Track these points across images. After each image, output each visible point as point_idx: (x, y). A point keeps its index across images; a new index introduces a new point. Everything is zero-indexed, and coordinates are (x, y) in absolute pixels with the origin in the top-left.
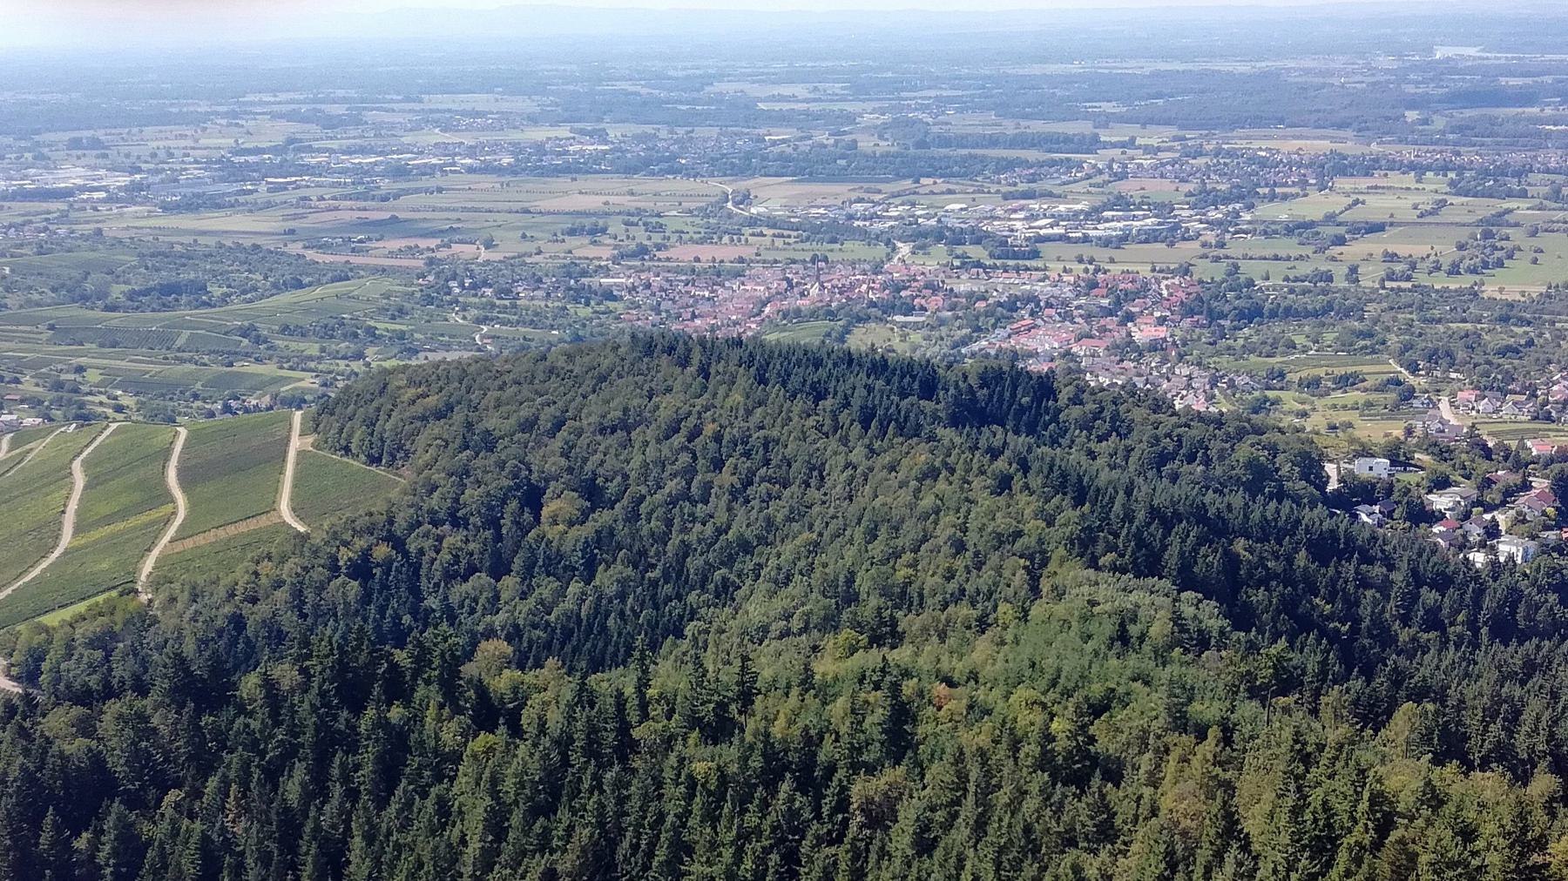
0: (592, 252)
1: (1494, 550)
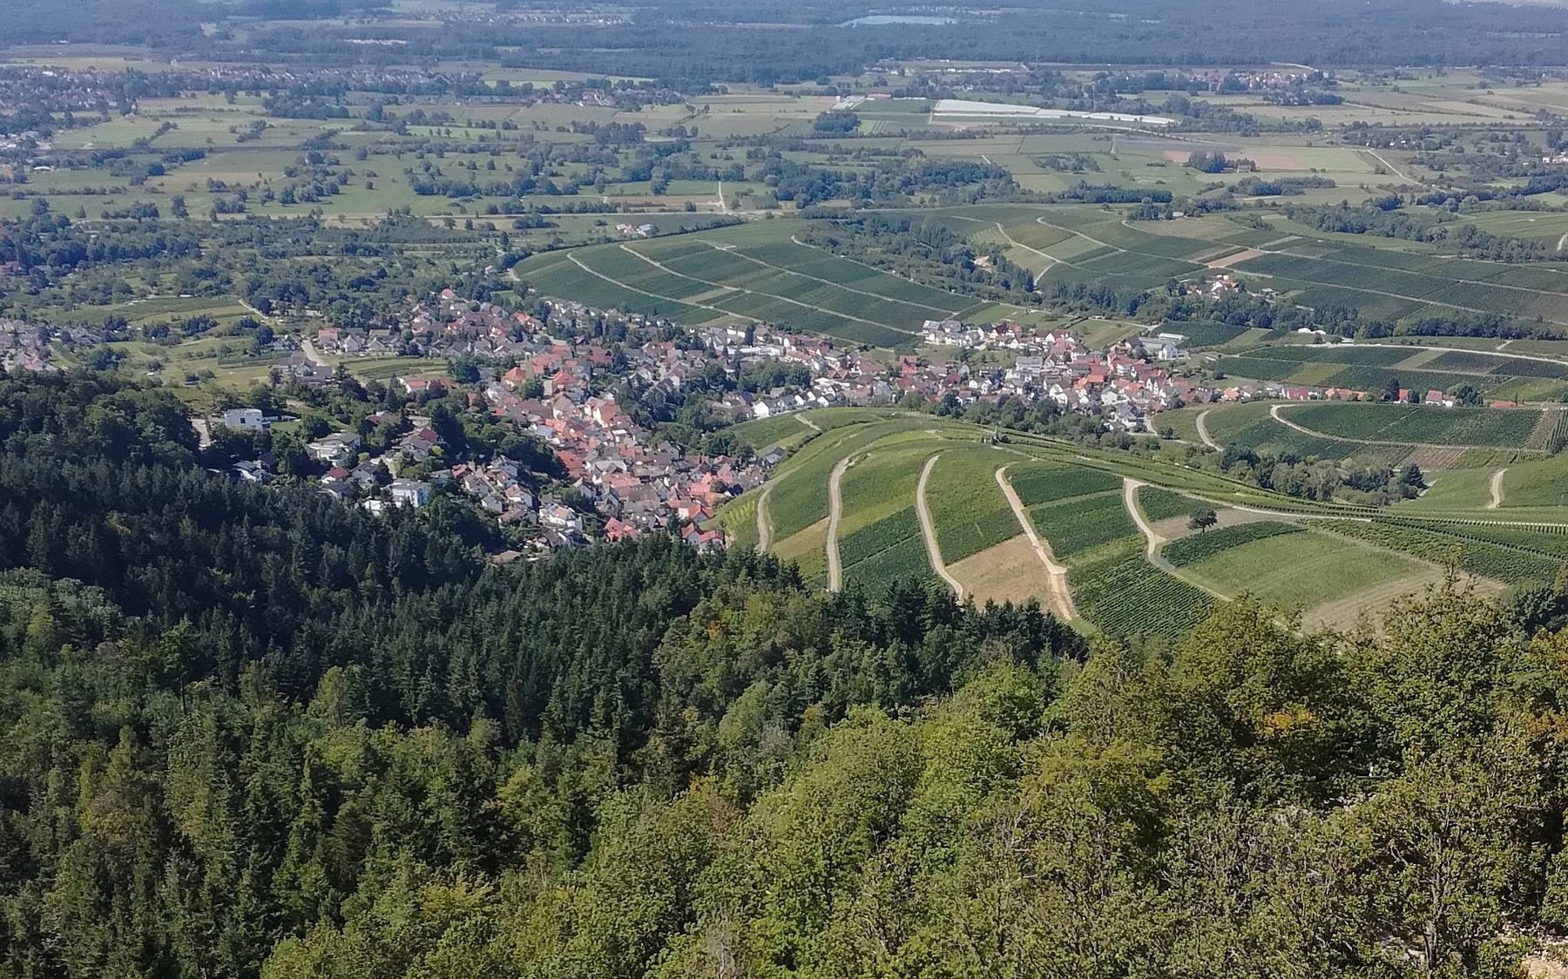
1: (388, 496)
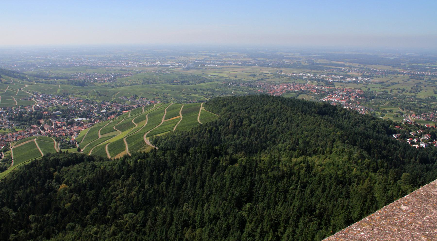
0: (253, 79)
1: (419, 145)
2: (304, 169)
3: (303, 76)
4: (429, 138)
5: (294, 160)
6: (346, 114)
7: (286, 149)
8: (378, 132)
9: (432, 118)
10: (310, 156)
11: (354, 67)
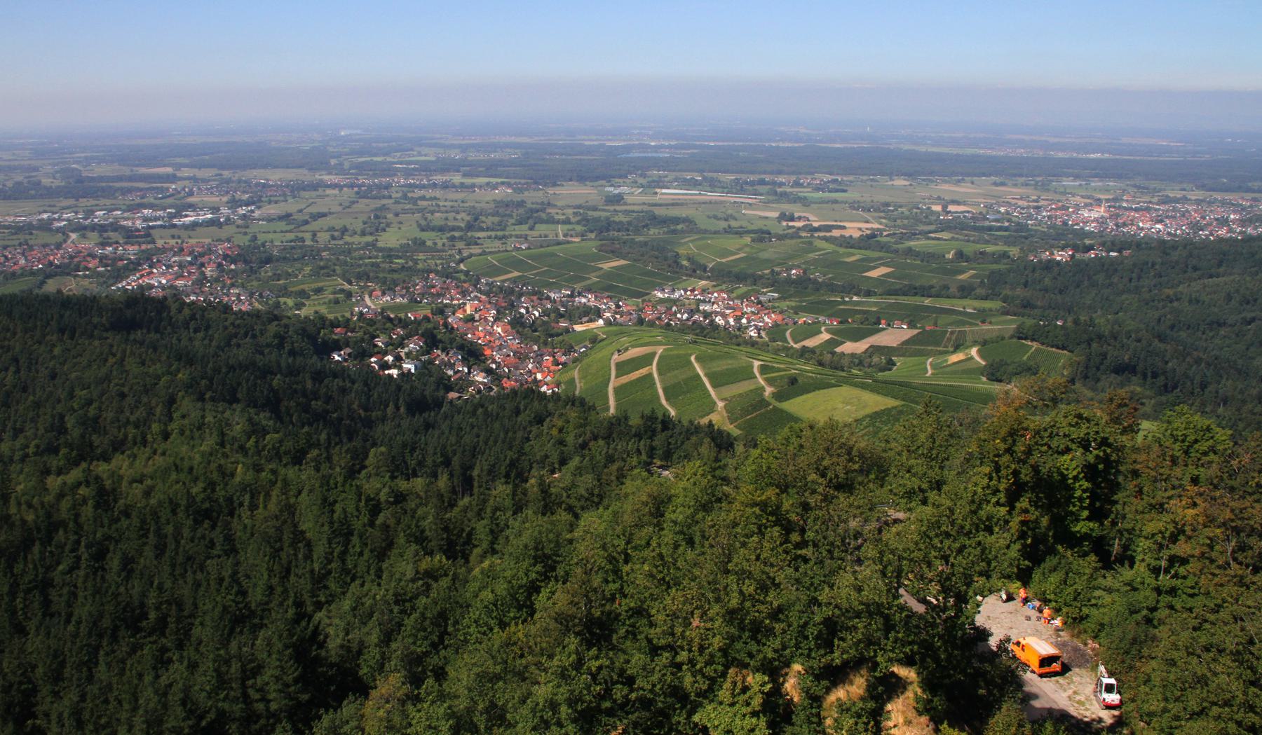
1: (400, 368)
2: (90, 503)
3: (51, 220)
4: (421, 347)
5: (54, 482)
6: (198, 316)
7: (27, 455)
8: (292, 353)
9: (423, 295)
10: (106, 458)
11: (205, 181)
